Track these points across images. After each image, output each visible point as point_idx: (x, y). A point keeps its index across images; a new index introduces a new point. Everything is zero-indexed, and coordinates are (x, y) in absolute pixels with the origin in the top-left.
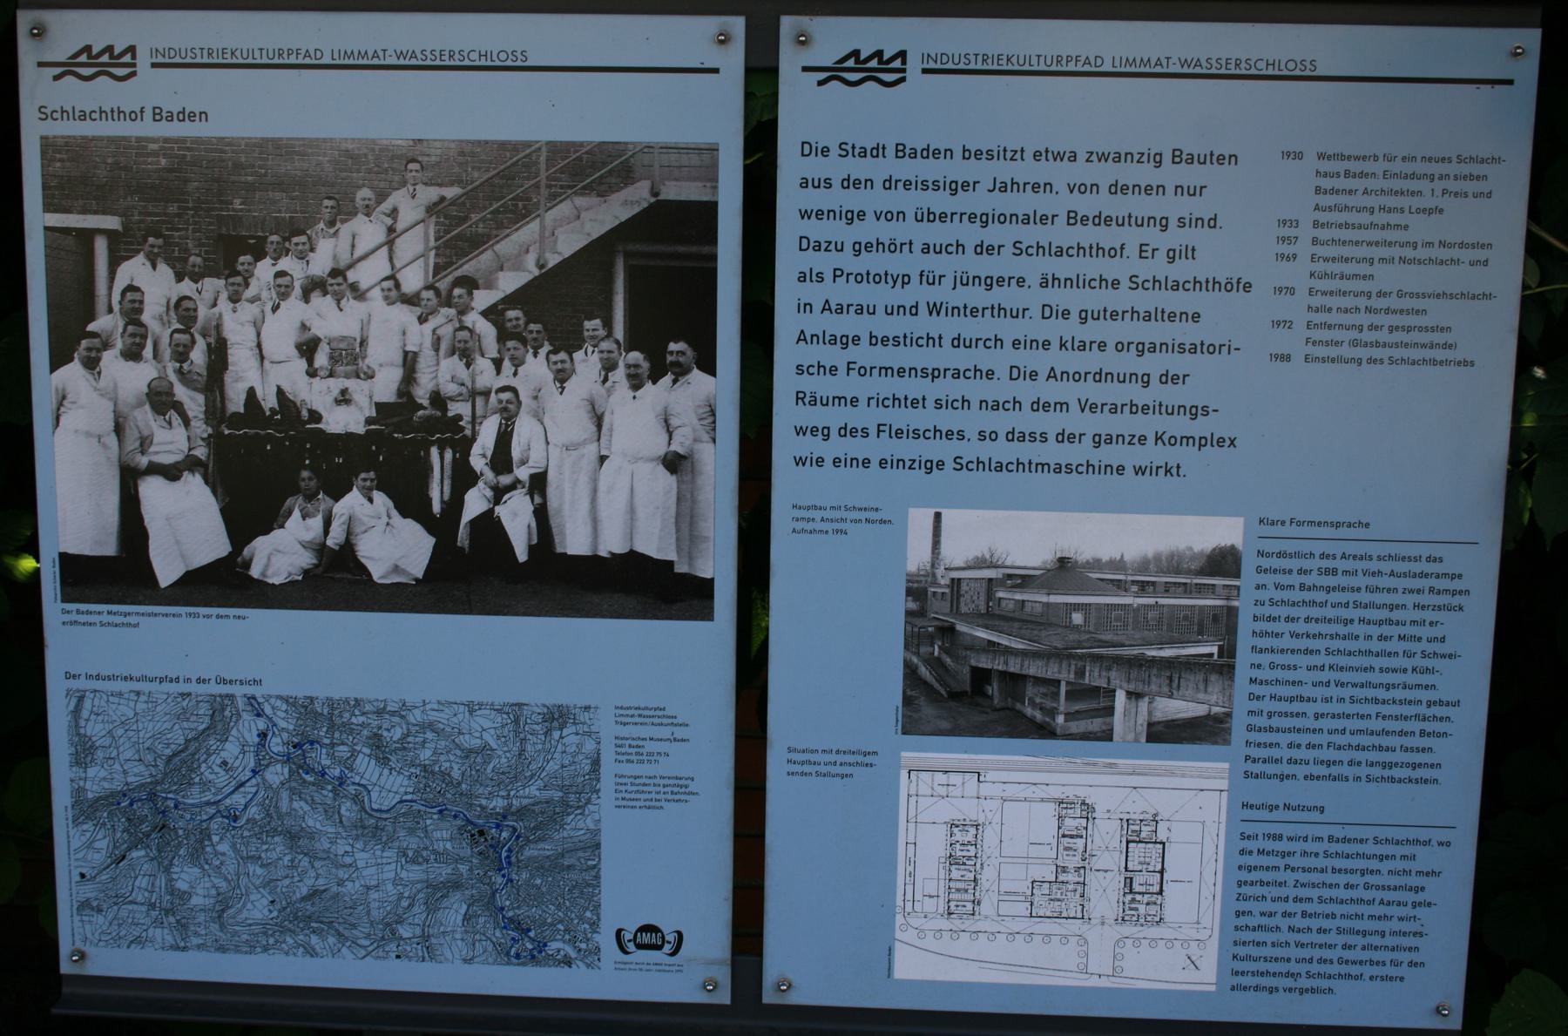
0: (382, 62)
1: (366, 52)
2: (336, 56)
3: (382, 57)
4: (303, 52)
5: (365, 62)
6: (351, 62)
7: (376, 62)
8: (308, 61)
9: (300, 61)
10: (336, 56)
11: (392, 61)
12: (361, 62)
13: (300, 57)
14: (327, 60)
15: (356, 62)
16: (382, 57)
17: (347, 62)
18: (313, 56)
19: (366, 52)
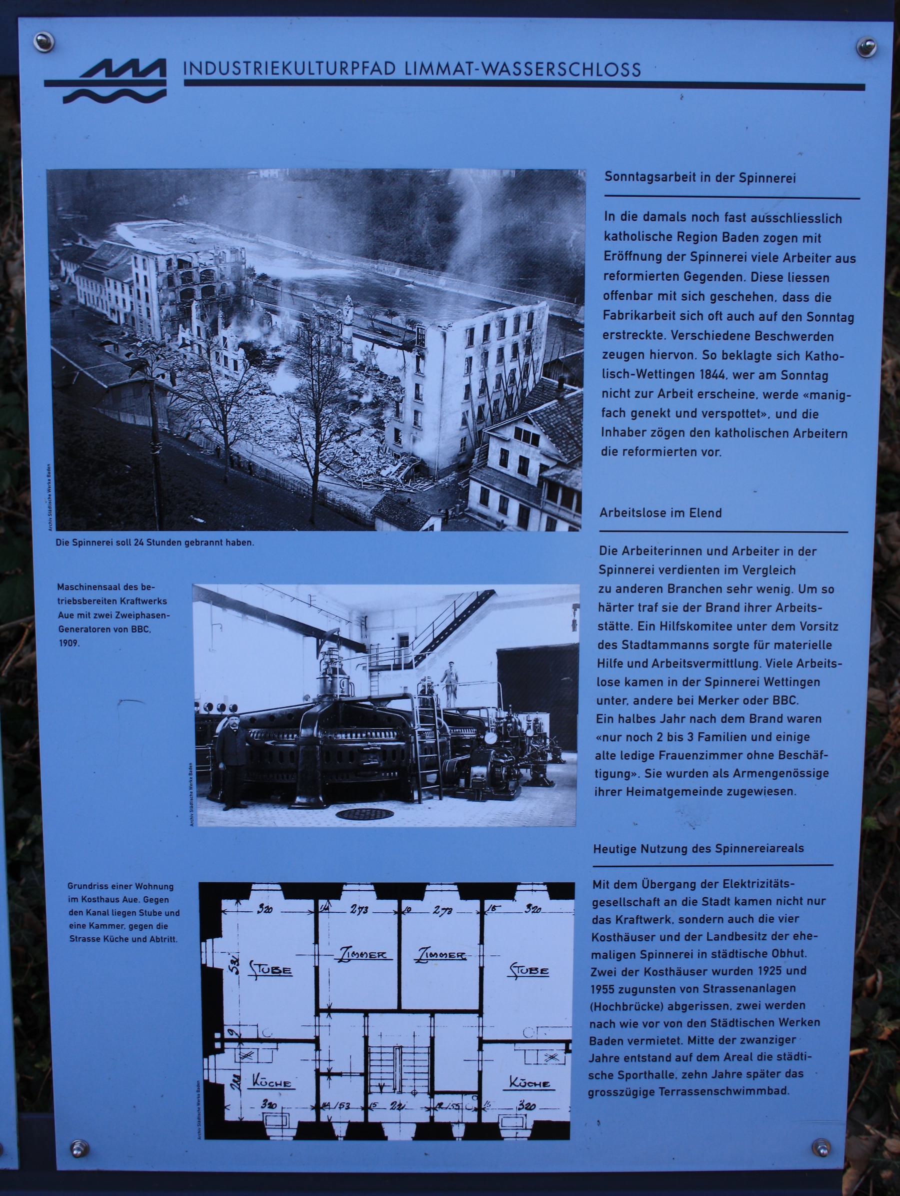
0: (467, 77)
1: (447, 65)
2: (411, 69)
3: (466, 71)
4: (371, 65)
5: (446, 77)
6: (429, 77)
7: (459, 76)
8: (376, 76)
9: (367, 76)
10: (411, 69)
11: (480, 75)
12: (440, 77)
13: (368, 71)
14: (400, 75)
15: (435, 77)
16: (466, 71)
17: (424, 76)
18: (383, 71)
19: (447, 65)
